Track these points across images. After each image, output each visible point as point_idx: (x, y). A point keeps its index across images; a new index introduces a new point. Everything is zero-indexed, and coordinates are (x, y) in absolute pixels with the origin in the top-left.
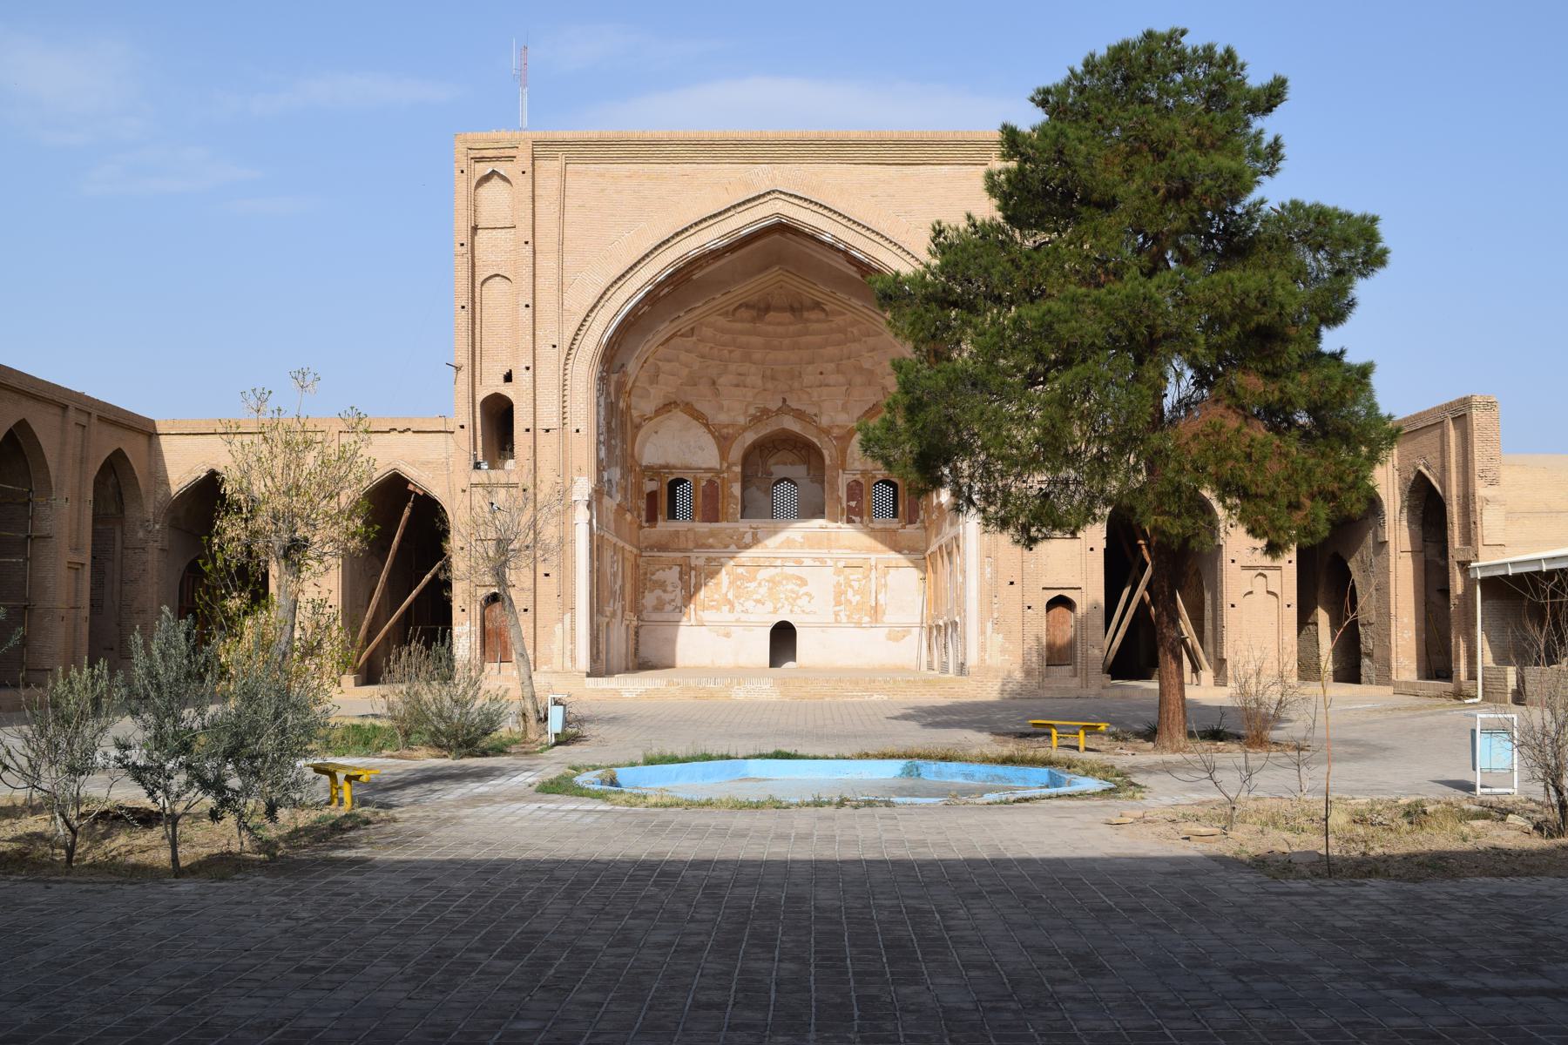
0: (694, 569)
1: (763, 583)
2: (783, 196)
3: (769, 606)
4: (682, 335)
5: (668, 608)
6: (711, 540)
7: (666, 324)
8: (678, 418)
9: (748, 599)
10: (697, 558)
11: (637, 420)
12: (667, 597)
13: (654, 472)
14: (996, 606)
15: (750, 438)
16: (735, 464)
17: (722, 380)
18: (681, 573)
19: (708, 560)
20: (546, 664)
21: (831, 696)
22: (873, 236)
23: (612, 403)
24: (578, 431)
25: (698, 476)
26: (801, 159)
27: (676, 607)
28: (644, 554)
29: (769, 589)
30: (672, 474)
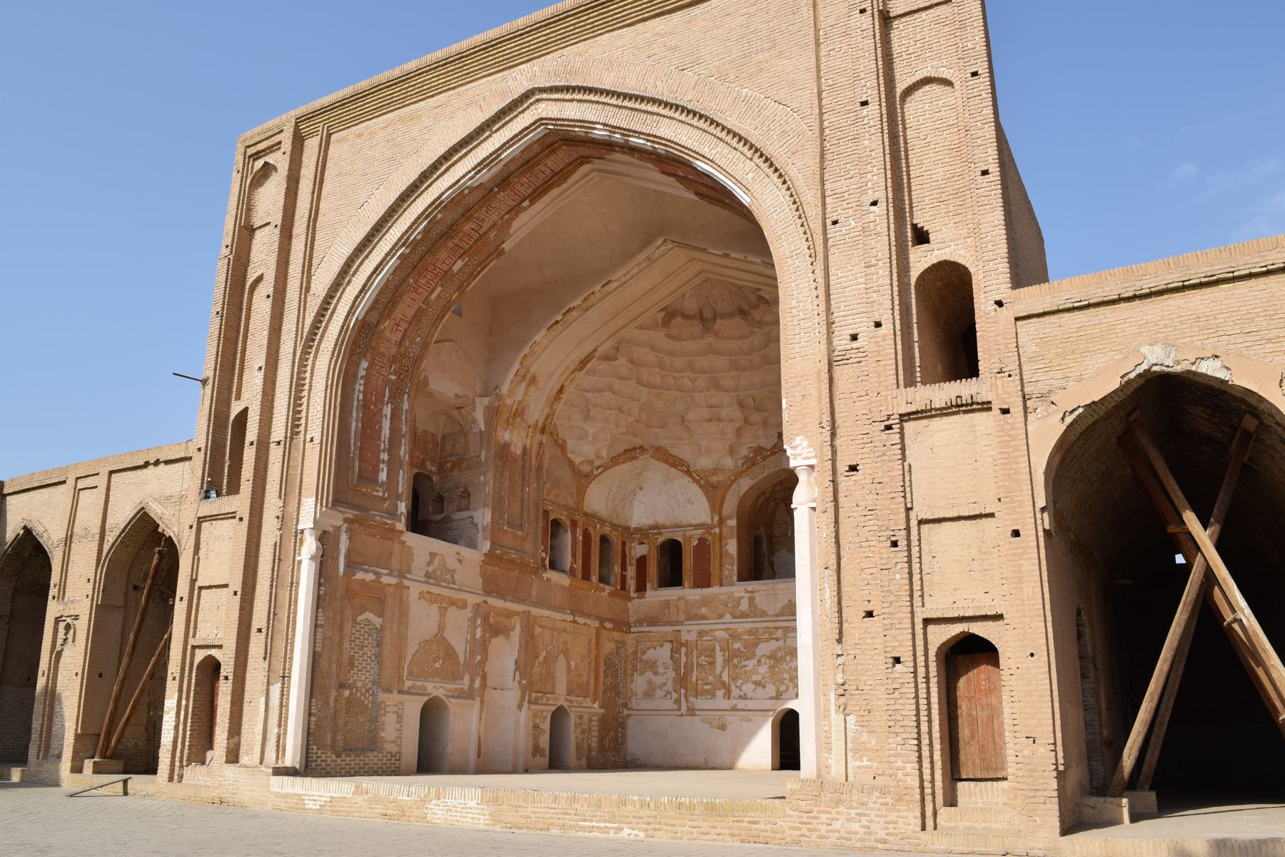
0: (686, 644)
1: (763, 660)
2: (544, 96)
3: (771, 690)
4: (607, 358)
5: (659, 693)
6: (703, 610)
7: (543, 332)
8: (656, 470)
9: (746, 682)
10: (689, 632)
11: (586, 468)
12: (658, 680)
13: (644, 534)
14: (840, 660)
15: (745, 484)
16: (730, 517)
17: (691, 416)
18: (672, 650)
19: (701, 634)
20: (247, 754)
21: (563, 827)
22: (649, 108)
23: (481, 432)
24: (312, 440)
25: (688, 534)
26: (563, 42)
27: (668, 693)
28: (633, 630)
29: (771, 667)
30: (660, 534)
